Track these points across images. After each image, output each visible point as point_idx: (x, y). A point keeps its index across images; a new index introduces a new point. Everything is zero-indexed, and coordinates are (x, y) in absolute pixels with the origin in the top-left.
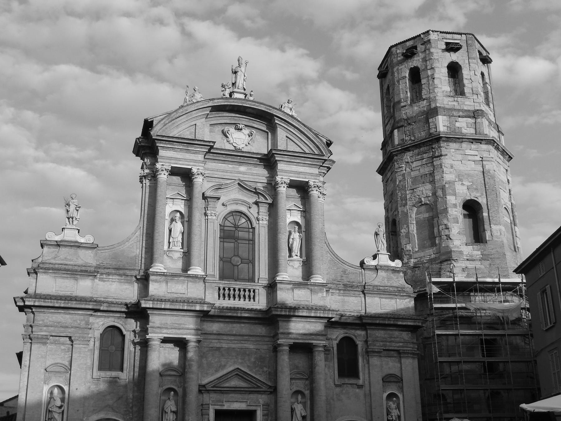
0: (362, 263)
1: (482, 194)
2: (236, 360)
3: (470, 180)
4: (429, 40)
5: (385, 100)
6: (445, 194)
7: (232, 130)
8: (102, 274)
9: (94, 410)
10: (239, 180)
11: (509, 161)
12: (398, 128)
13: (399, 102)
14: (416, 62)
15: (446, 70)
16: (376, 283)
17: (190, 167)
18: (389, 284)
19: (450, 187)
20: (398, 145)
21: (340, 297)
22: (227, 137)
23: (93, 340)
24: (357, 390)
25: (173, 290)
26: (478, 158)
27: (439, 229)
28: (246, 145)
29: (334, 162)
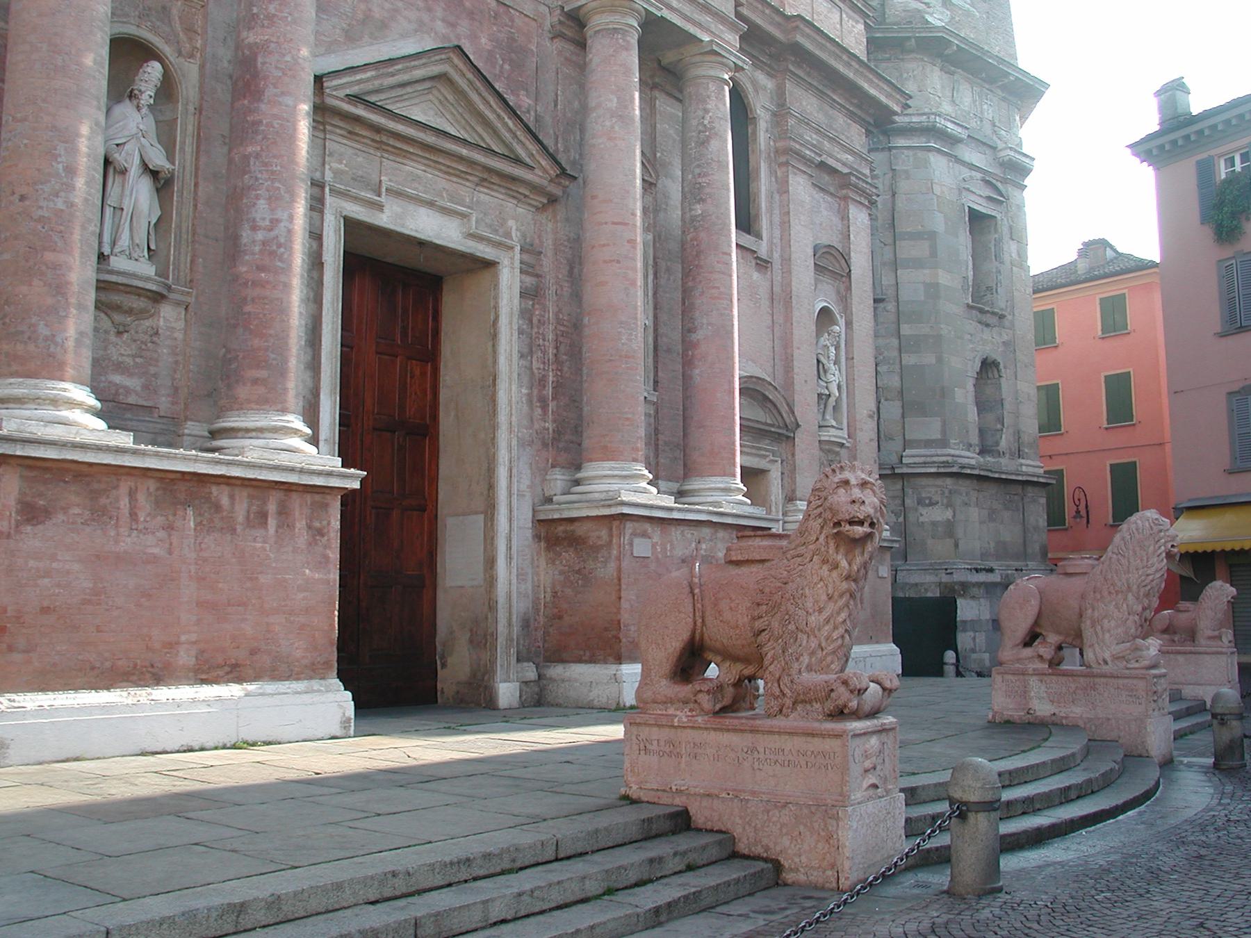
2: (426, 17)
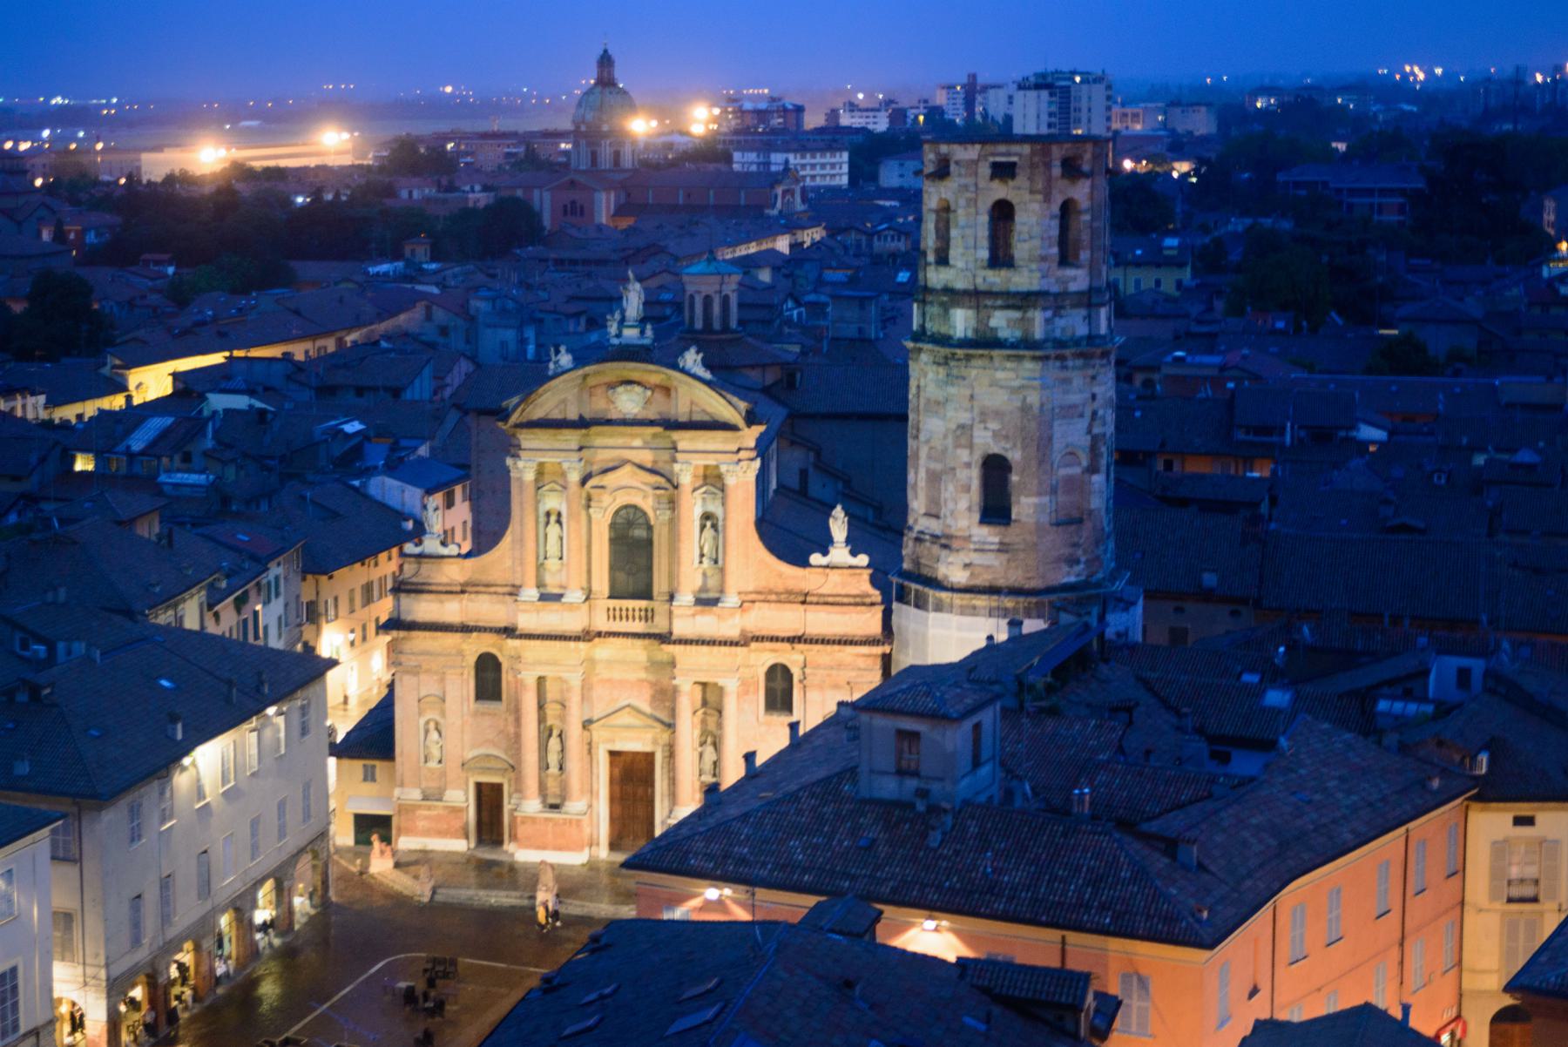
1: (1015, 445)
15: (984, 219)
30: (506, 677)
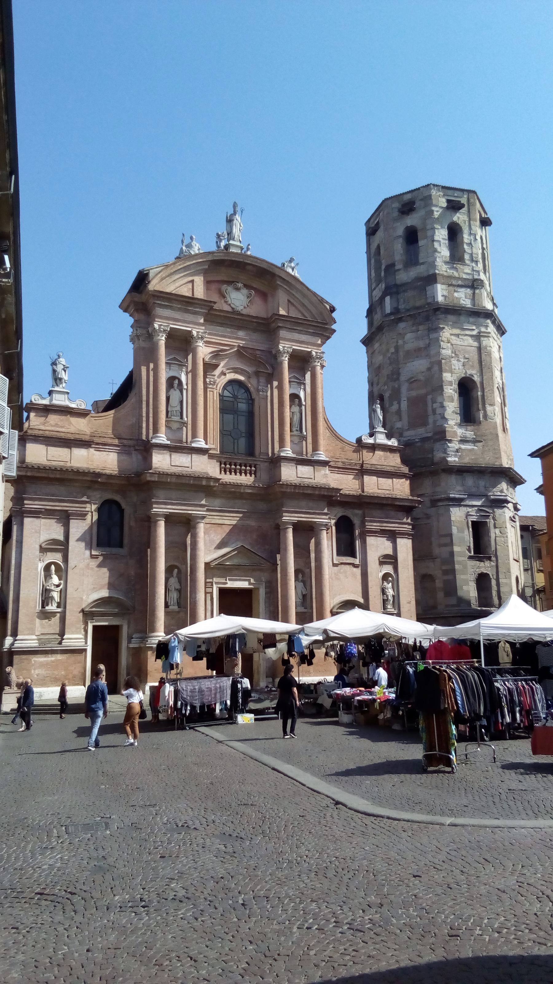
0: (359, 440)
3: (467, 356)
4: (430, 196)
5: (373, 261)
6: (441, 371)
7: (230, 289)
8: (98, 444)
9: (94, 588)
10: (239, 346)
11: (501, 336)
12: (391, 294)
13: (393, 265)
14: (412, 220)
16: (373, 462)
17: (190, 329)
18: (385, 464)
19: (446, 363)
20: (391, 314)
21: (338, 475)
22: (224, 297)
23: (90, 514)
24: (355, 569)
25: (177, 464)
26: (474, 333)
27: (432, 406)
28: (245, 308)
29: (334, 331)
30: (130, 521)
